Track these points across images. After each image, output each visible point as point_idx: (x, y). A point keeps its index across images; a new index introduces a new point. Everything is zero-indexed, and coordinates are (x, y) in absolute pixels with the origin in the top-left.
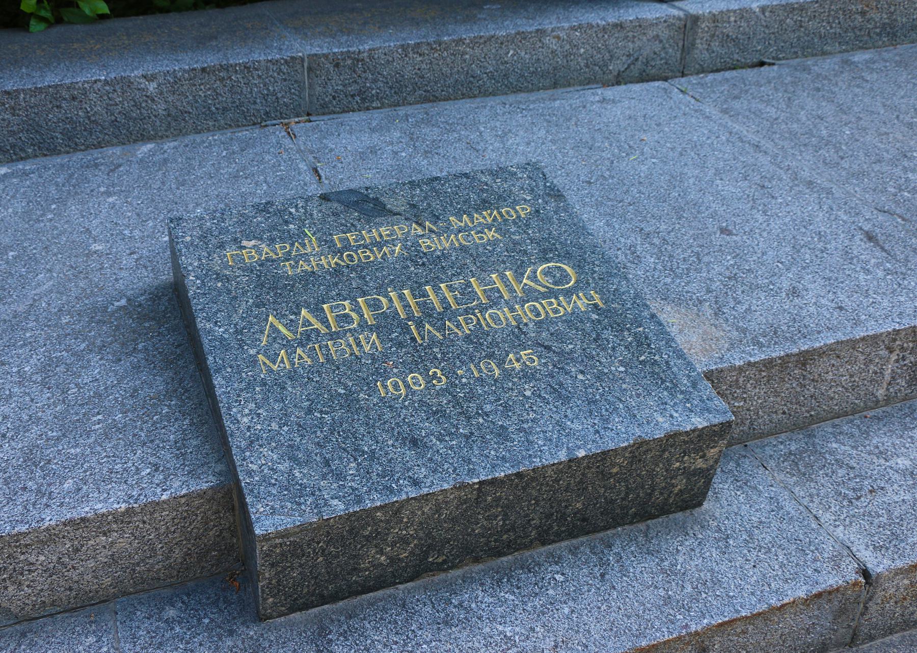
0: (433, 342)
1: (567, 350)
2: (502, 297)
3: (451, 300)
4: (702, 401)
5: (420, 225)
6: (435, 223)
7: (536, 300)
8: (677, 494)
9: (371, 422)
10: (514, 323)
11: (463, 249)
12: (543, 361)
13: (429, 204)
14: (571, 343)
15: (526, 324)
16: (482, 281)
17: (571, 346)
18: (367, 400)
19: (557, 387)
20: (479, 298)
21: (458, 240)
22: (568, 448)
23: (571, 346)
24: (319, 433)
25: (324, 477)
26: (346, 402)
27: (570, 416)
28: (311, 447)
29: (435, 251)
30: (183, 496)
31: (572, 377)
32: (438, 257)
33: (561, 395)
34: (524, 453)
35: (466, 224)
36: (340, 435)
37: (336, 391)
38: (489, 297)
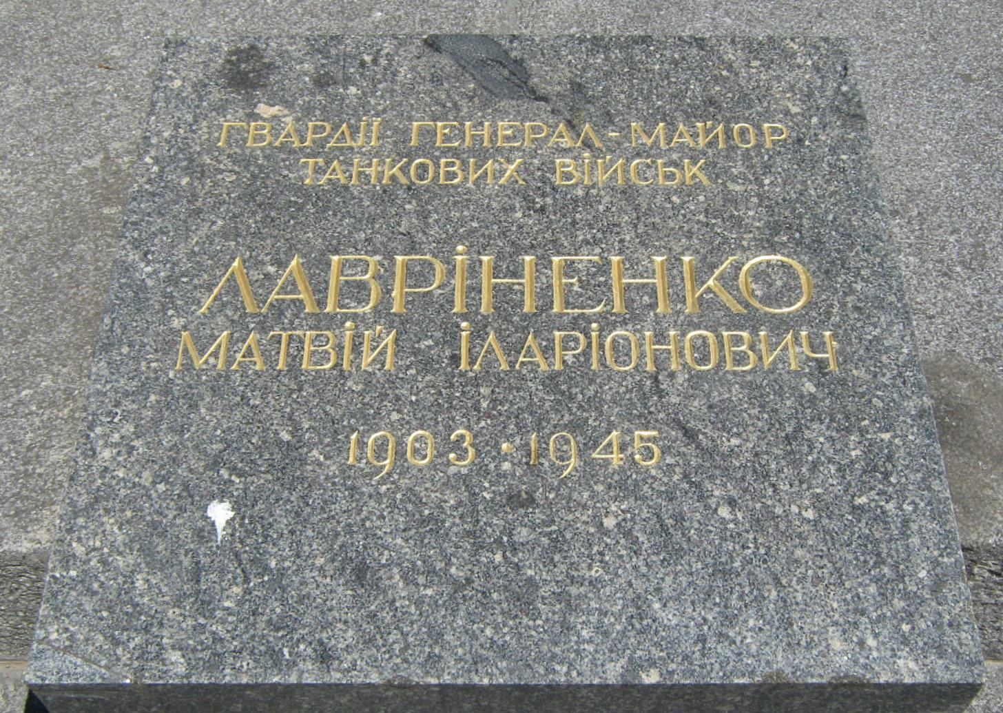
0: (488, 373)
1: (725, 449)
2: (653, 306)
5: (571, 125)
9: (308, 510)
10: (650, 367)
11: (628, 193)
12: (669, 460)
13: (607, 91)
14: (738, 435)
15: (672, 375)
16: (631, 265)
17: (735, 441)
18: (320, 465)
19: (670, 522)
20: (610, 301)
21: (626, 171)
23: (735, 441)
25: (178, 603)
28: (186, 534)
29: (575, 186)
31: (707, 507)
32: (575, 200)
33: (669, 541)
34: (545, 648)
35: (656, 144)
36: (241, 525)
37: (276, 433)
38: (628, 303)
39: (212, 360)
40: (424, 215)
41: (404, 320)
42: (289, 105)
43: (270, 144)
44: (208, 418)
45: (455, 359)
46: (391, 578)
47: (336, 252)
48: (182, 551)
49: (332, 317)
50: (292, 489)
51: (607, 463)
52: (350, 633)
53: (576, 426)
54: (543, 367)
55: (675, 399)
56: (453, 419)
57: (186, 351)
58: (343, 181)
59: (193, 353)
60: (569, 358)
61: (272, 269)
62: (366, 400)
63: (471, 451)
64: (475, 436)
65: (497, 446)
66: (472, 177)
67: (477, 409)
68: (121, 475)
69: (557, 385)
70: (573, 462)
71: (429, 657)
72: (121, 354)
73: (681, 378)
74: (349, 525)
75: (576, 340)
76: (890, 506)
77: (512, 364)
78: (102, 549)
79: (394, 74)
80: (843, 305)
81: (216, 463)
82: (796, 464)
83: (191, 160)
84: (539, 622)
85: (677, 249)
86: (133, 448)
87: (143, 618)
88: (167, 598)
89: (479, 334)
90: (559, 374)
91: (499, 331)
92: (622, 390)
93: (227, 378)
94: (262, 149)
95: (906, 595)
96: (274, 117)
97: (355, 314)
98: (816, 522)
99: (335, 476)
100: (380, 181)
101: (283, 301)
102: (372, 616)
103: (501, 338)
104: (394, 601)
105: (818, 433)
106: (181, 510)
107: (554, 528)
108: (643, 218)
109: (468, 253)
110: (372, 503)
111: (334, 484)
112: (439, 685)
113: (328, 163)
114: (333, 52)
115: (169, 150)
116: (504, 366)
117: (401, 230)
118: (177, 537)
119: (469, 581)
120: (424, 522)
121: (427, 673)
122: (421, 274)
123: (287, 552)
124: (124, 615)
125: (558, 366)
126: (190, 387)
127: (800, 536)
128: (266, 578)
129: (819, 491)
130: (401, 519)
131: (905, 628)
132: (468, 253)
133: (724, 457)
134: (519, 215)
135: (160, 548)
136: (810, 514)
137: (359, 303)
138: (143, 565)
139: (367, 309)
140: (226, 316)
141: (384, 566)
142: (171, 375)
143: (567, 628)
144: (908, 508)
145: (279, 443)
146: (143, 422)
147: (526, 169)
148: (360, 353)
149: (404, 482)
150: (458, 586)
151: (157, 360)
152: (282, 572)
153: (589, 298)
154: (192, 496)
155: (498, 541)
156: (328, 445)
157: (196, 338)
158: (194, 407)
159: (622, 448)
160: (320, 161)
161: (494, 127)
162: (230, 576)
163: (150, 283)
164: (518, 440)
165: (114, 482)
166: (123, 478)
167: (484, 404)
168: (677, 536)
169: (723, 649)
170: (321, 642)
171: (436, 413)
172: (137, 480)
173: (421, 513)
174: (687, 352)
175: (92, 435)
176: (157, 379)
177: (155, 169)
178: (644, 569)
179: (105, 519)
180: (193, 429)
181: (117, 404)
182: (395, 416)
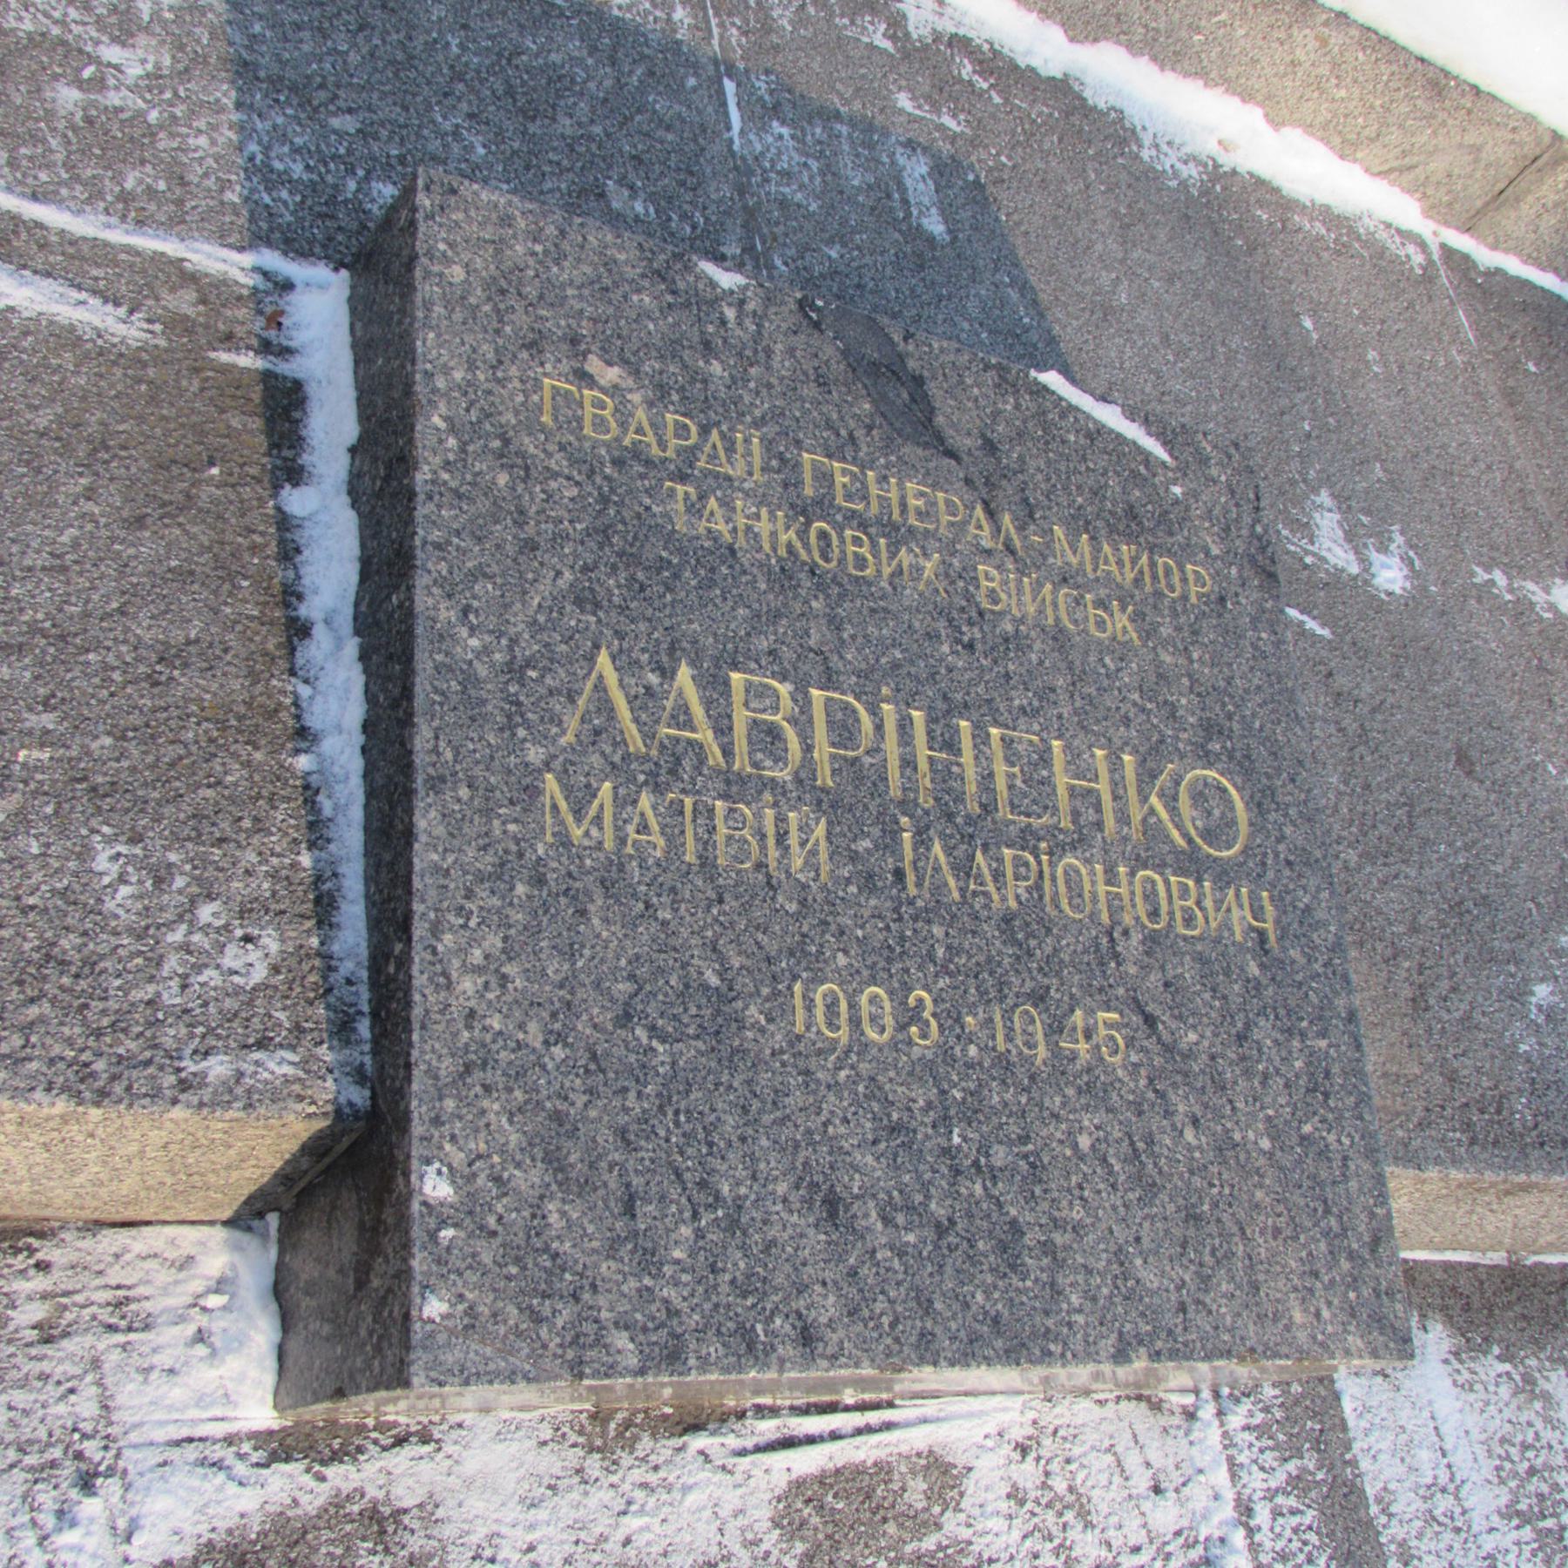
1: (1183, 1046)
2: (1099, 825)
3: (1001, 784)
6: (1021, 528)
10: (1105, 918)
11: (1059, 637)
12: (1134, 1058)
13: (1021, 458)
14: (1194, 1027)
16: (1073, 755)
17: (1192, 1037)
18: (762, 1030)
19: (1141, 1145)
20: (1055, 809)
23: (1192, 1037)
24: (632, 1095)
25: (611, 1252)
26: (714, 1017)
28: (605, 1136)
31: (1173, 1125)
38: (1076, 814)
39: (594, 832)
40: (835, 624)
43: (617, 439)
44: (605, 934)
45: (899, 874)
46: (866, 1216)
47: (735, 666)
48: (604, 1165)
49: (742, 780)
50: (733, 1070)
51: (1074, 1057)
52: (832, 1299)
53: (1039, 998)
56: (907, 971)
57: (555, 807)
58: (728, 538)
60: (1024, 896)
62: (805, 929)
64: (935, 1001)
65: (958, 1020)
67: (931, 957)
68: (497, 1026)
69: (1013, 933)
70: (1042, 1052)
71: (922, 1335)
72: (459, 800)
73: (1136, 938)
74: (809, 1132)
75: (1026, 864)
76: (1331, 1138)
78: (489, 1156)
79: (769, 353)
80: (1277, 855)
81: (628, 1016)
82: (1248, 1073)
84: (1029, 1283)
85: (1118, 742)
86: (504, 977)
87: (568, 1276)
88: (595, 1244)
89: (921, 841)
92: (1080, 948)
94: (607, 445)
95: (1351, 1256)
96: (616, 386)
97: (773, 779)
98: (1270, 1155)
99: (782, 1052)
100: (775, 550)
101: (677, 740)
102: (853, 1273)
104: (874, 1251)
105: (1264, 1031)
107: (1030, 1147)
110: (832, 1098)
111: (784, 1064)
113: (702, 497)
115: (468, 410)
116: (956, 895)
117: (812, 643)
118: (594, 1140)
120: (894, 1129)
123: (741, 1173)
125: (1013, 904)
126: (570, 875)
128: (720, 1213)
129: (1270, 1112)
130: (868, 1125)
131: (1352, 1295)
134: (945, 648)
135: (573, 1158)
136: (1265, 1144)
137: (776, 761)
138: (554, 1187)
140: (603, 753)
141: (857, 1197)
142: (541, 852)
144: (1346, 1141)
145: (705, 987)
146: (513, 931)
147: (945, 572)
148: (788, 848)
150: (941, 1230)
151: (516, 821)
153: (1034, 802)
154: (603, 1071)
155: (976, 1164)
156: (767, 999)
157: (568, 790)
161: (901, 485)
162: (674, 1208)
165: (488, 1037)
166: (500, 1033)
167: (940, 952)
171: (889, 960)
172: (521, 1036)
173: (889, 1115)
175: (440, 948)
176: (521, 855)
177: (452, 442)
178: (1122, 1210)
179: (485, 1103)
180: (587, 952)
181: (470, 894)
182: (842, 960)
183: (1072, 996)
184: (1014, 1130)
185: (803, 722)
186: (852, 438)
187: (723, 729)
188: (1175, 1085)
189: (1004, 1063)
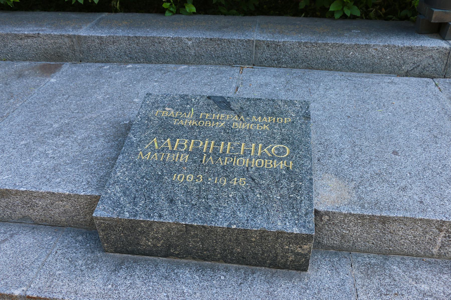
1: (261, 183)
2: (250, 154)
4: (305, 222)
5: (239, 116)
7: (264, 159)
8: (291, 261)
10: (247, 166)
12: (247, 184)
15: (252, 168)
16: (247, 145)
17: (264, 182)
18: (166, 179)
22: (230, 223)
23: (264, 182)
27: (241, 210)
30: (89, 196)
31: (254, 194)
32: (236, 131)
33: (244, 201)
38: (244, 153)
41: (191, 153)
42: (173, 108)
45: (202, 161)
51: (232, 184)
53: (226, 176)
54: (222, 164)
55: (251, 173)
59: (142, 155)
60: (228, 163)
61: (163, 141)
63: (202, 179)
65: (208, 179)
66: (213, 125)
77: (214, 163)
79: (199, 103)
83: (148, 118)
89: (208, 156)
90: (225, 166)
91: (213, 156)
93: (149, 161)
103: (213, 157)
106: (134, 186)
108: (252, 136)
109: (209, 140)
112: (185, 224)
113: (180, 120)
114: (185, 98)
116: (213, 163)
119: (196, 204)
120: (188, 192)
121: (183, 221)
122: (197, 144)
124: (117, 204)
125: (225, 164)
127: (275, 202)
132: (209, 140)
133: (260, 185)
136: (279, 198)
139: (183, 150)
143: (216, 215)
149: (185, 184)
152: (154, 199)
155: (204, 198)
157: (143, 153)
158: (140, 166)
159: (237, 181)
160: (178, 120)
163: (135, 141)
164: (213, 178)
167: (206, 170)
168: (246, 200)
169: (252, 223)
170: (160, 213)
174: (256, 163)
178: (237, 205)
181: (123, 164)
182: (185, 171)
183: (235, 176)
184: (215, 193)
185: (188, 145)
186: (212, 111)
187: (173, 146)
188: (257, 189)
189: (216, 184)
